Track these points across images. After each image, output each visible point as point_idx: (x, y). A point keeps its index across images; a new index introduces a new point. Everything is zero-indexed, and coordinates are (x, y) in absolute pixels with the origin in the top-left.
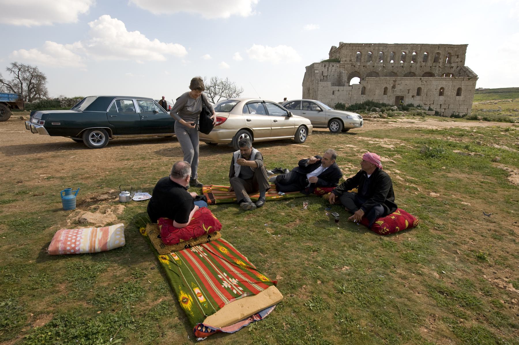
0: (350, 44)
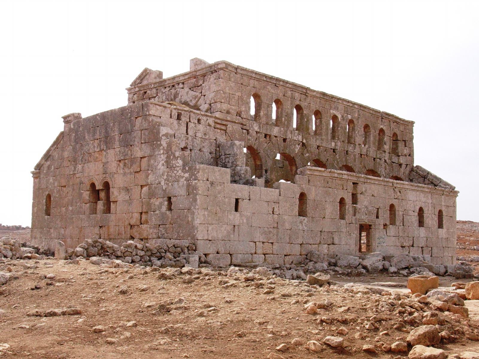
0: (237, 68)
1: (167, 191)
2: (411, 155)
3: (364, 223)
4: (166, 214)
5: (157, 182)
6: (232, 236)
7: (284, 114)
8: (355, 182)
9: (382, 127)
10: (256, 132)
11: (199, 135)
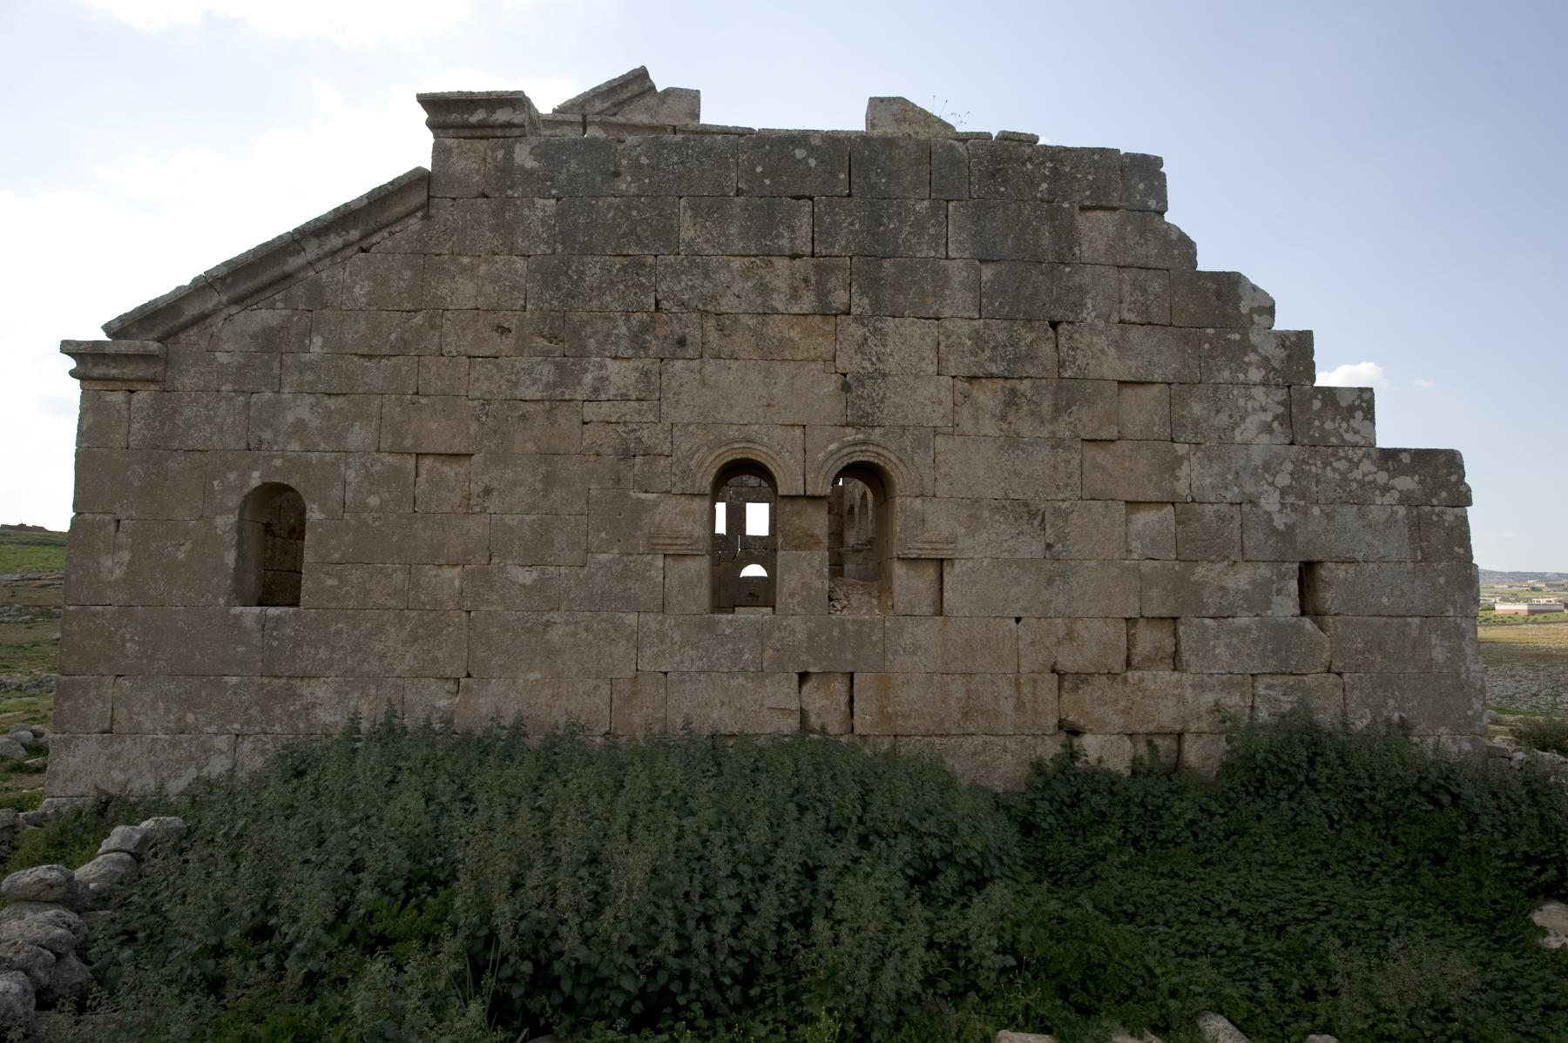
1: (1300, 538)
4: (1300, 630)
5: (1233, 494)
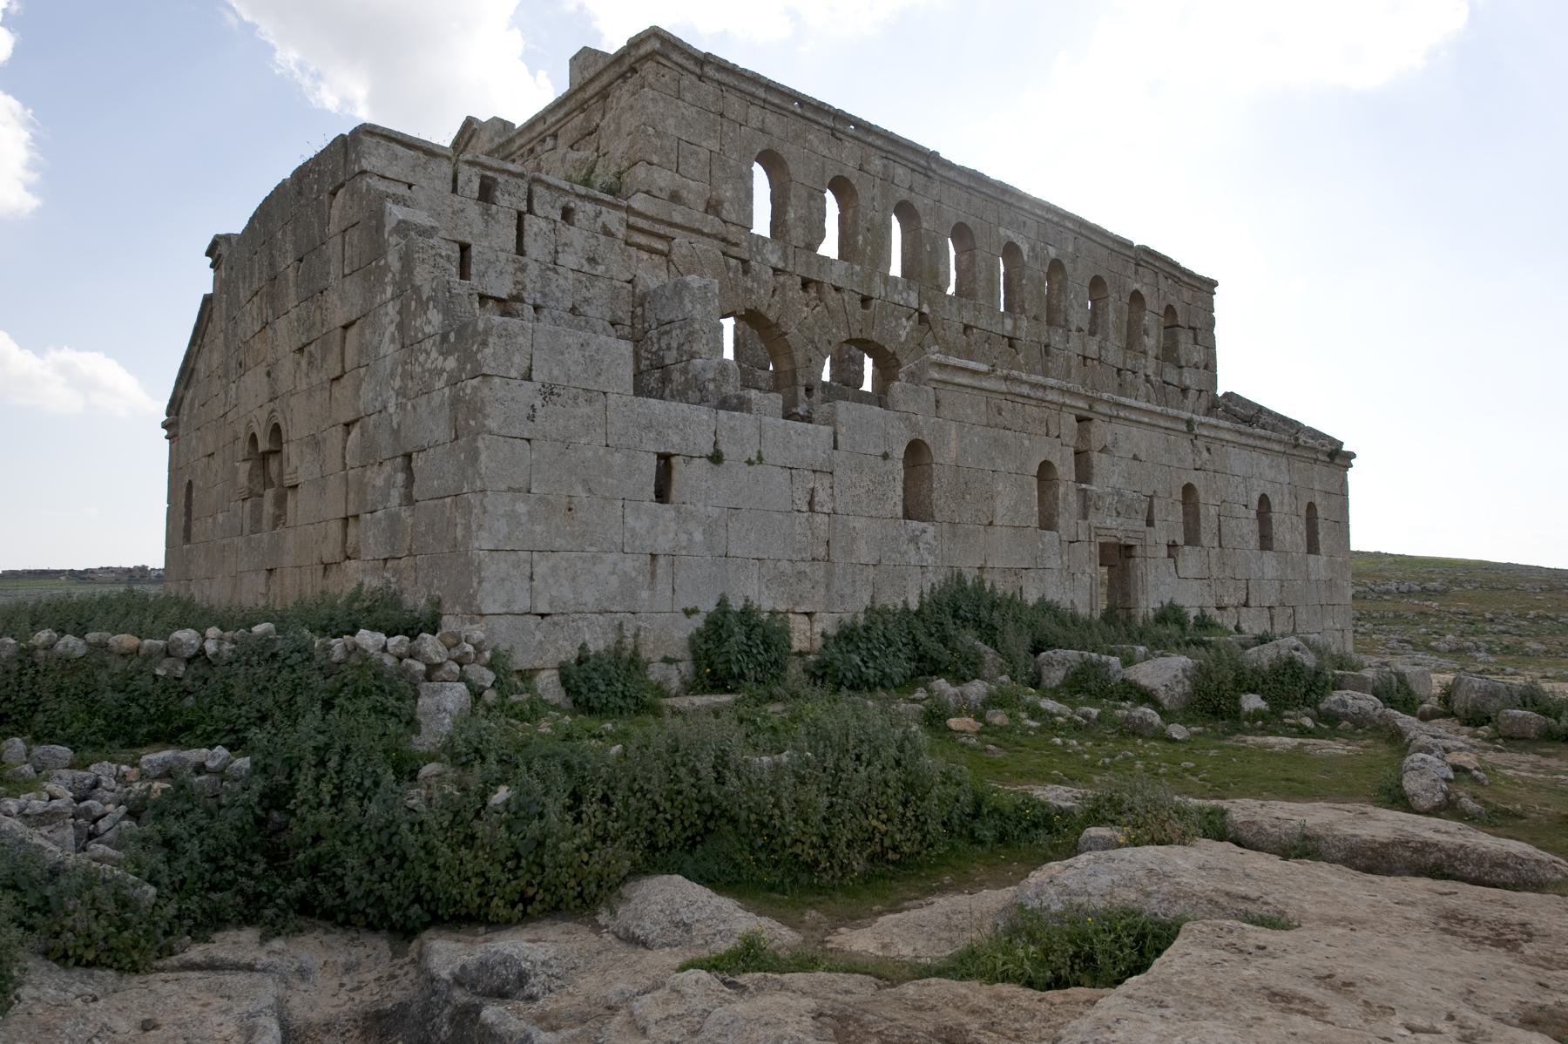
2: (1210, 366)
3: (1113, 540)
6: (645, 594)
7: (862, 224)
8: (1085, 414)
9: (1137, 286)
10: (775, 270)
11: (569, 260)
